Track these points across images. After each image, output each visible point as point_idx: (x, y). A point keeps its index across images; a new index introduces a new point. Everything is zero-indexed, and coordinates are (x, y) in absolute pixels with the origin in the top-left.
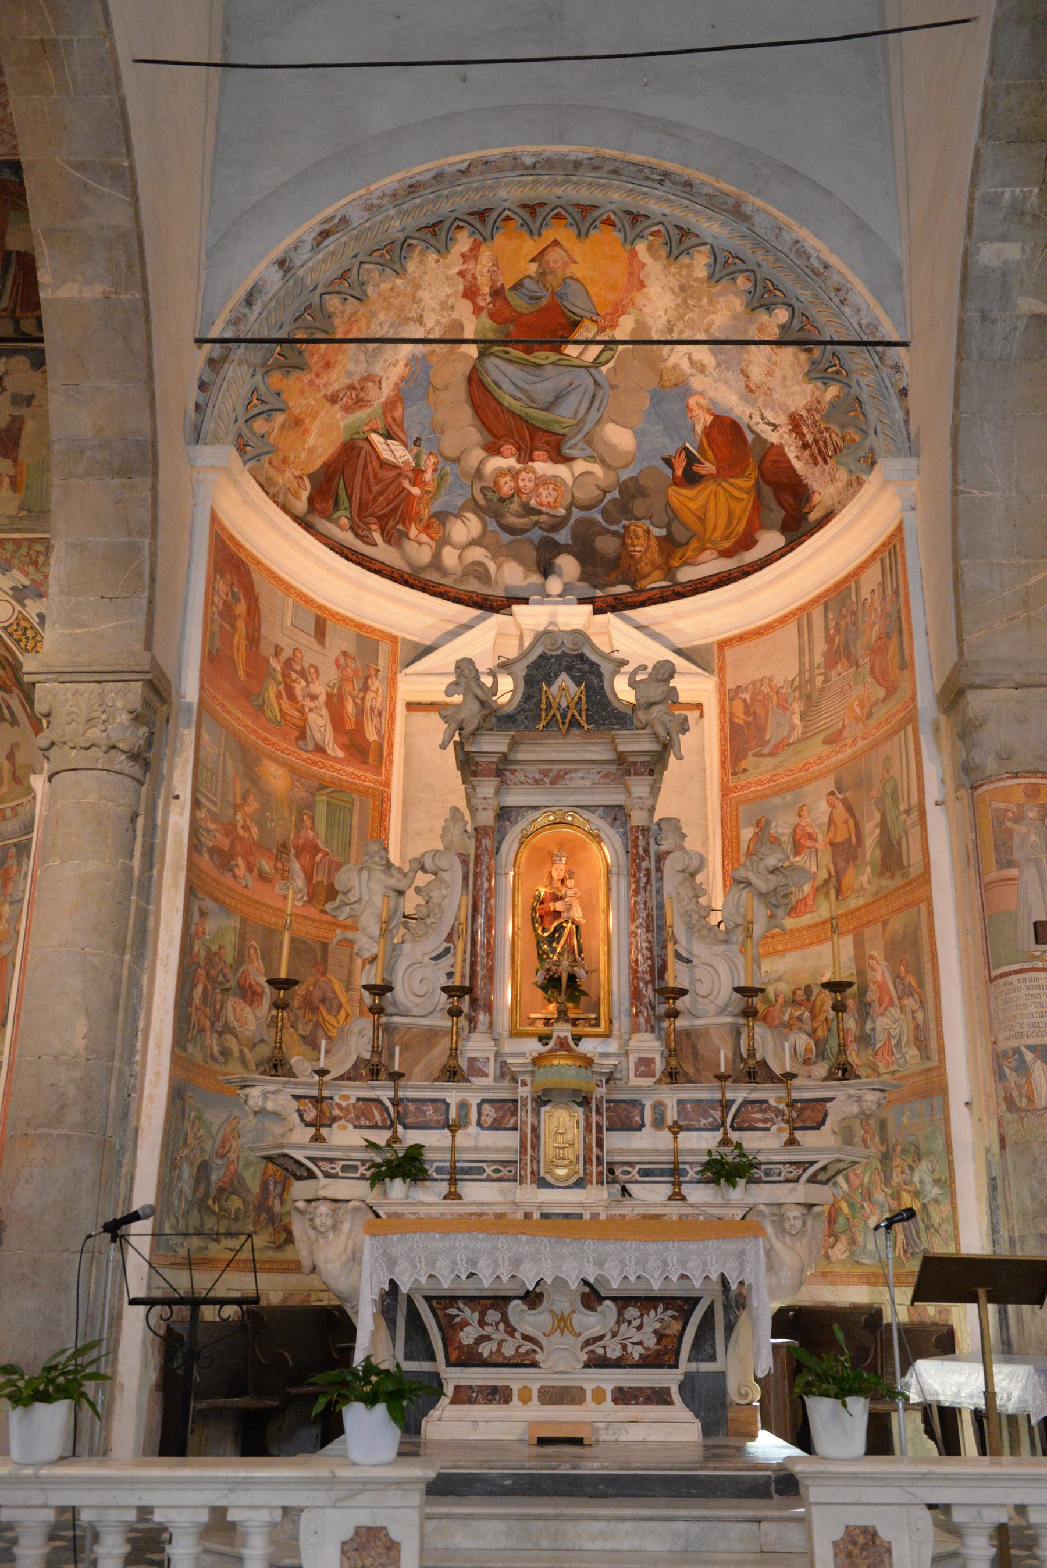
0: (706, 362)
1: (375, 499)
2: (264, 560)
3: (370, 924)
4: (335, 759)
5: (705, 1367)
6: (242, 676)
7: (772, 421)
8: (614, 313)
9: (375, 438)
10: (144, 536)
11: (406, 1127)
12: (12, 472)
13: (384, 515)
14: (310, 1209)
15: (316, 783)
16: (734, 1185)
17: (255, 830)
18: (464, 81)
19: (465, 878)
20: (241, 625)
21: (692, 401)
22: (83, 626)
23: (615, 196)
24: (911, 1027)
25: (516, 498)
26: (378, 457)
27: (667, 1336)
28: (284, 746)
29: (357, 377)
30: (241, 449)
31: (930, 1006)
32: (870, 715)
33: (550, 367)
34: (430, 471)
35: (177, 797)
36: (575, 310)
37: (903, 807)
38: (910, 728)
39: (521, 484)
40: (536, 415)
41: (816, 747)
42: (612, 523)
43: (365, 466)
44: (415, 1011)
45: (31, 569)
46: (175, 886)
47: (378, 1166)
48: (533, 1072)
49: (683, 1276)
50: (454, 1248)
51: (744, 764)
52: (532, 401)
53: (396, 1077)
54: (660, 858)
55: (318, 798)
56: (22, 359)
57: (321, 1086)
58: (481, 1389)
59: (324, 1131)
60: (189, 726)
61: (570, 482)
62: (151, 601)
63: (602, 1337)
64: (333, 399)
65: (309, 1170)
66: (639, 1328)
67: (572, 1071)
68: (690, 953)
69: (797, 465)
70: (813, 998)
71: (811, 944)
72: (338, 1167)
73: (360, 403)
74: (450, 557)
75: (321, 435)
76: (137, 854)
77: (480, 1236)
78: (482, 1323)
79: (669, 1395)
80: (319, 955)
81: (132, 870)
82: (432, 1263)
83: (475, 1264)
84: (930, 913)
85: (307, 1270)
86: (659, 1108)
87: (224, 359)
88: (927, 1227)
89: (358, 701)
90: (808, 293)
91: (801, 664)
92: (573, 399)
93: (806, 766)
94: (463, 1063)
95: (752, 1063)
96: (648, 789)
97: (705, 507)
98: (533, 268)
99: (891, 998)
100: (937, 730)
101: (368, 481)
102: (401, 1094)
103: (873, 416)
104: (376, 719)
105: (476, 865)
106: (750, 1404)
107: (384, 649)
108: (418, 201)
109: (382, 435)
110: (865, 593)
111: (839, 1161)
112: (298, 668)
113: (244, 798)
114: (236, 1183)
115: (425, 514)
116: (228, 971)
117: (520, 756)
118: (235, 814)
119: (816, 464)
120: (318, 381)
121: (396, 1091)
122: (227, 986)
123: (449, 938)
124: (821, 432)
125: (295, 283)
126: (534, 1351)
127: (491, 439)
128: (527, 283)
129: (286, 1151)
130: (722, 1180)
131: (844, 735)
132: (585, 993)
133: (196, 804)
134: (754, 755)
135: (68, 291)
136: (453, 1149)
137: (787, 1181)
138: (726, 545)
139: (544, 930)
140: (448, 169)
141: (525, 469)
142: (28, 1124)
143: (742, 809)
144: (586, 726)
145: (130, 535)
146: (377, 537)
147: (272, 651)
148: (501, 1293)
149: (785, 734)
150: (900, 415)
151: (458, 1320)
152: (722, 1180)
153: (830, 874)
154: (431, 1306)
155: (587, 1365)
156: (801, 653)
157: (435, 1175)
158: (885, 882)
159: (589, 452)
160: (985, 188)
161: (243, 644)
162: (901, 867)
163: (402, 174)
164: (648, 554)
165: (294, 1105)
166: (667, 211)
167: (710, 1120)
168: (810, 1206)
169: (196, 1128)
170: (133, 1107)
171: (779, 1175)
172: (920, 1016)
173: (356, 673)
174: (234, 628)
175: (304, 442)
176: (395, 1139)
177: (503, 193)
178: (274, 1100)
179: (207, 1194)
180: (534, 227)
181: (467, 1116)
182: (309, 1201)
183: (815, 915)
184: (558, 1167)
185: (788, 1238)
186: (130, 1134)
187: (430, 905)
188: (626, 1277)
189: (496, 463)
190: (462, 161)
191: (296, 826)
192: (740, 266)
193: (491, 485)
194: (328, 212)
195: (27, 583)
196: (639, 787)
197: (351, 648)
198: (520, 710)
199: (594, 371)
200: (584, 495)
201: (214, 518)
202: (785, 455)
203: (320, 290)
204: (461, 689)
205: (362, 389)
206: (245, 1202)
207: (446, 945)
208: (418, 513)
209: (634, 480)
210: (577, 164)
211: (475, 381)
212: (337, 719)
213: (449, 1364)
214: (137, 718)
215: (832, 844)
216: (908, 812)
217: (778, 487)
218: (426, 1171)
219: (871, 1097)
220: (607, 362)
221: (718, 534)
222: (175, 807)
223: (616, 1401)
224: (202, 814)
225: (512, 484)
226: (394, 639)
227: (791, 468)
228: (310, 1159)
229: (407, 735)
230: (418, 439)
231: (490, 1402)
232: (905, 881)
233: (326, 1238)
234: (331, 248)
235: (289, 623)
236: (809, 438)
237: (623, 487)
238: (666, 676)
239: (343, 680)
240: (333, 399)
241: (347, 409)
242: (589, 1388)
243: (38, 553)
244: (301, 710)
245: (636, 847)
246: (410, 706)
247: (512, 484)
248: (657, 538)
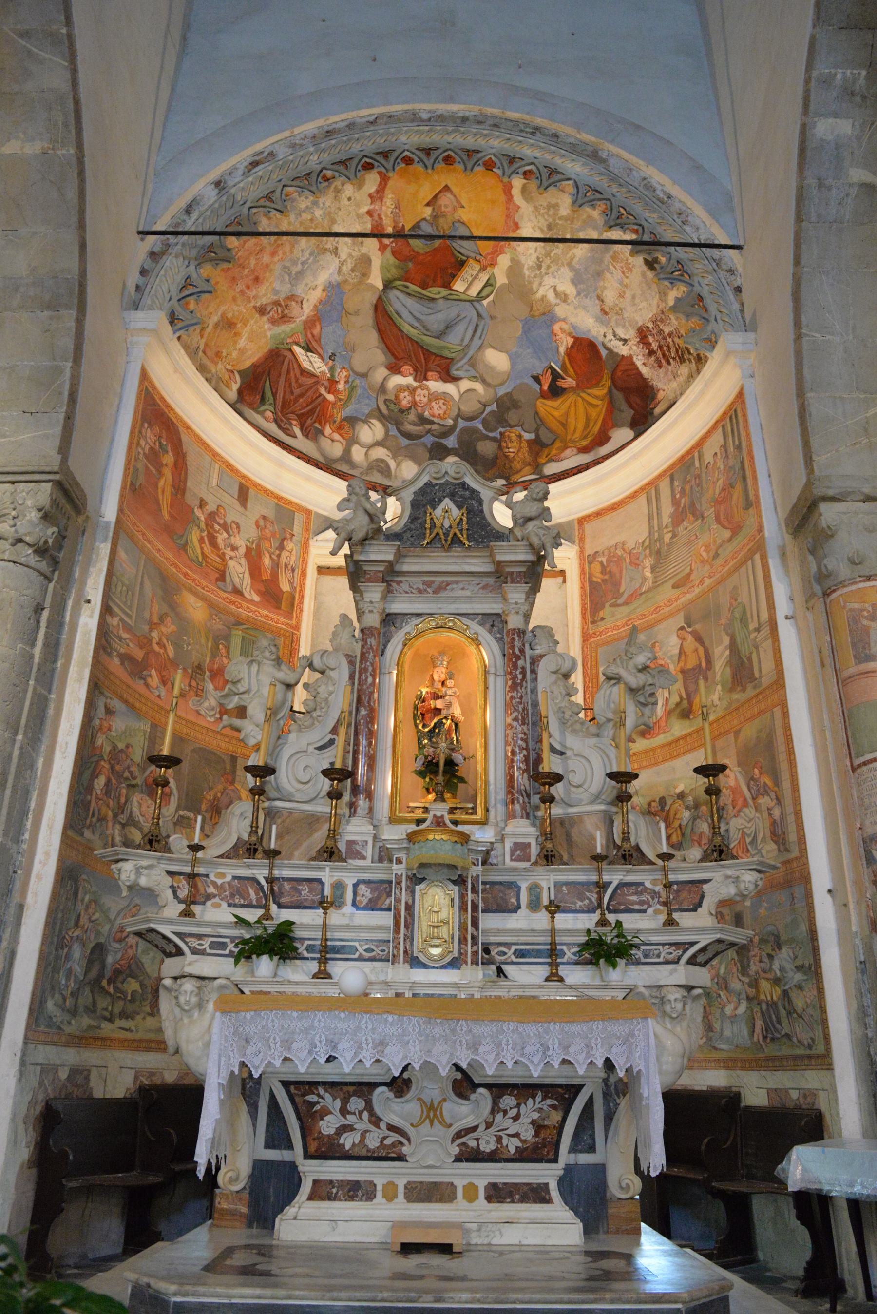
0: (568, 292)
1: (296, 400)
2: (194, 427)
3: (257, 712)
4: (251, 601)
5: (584, 1159)
6: (166, 516)
7: (623, 336)
8: (493, 253)
9: (297, 350)
11: (280, 906)
13: (303, 414)
14: (175, 987)
15: (232, 619)
16: (614, 966)
17: (171, 650)
18: (374, 60)
19: (352, 677)
20: (168, 473)
21: (556, 327)
23: (495, 143)
24: (767, 824)
25: (413, 410)
26: (299, 366)
27: (545, 1127)
28: (205, 583)
29: (282, 296)
30: (173, 319)
31: (788, 802)
32: (716, 556)
33: (441, 301)
34: (342, 382)
35: (89, 601)
36: (462, 251)
37: (752, 627)
38: (757, 557)
39: (417, 398)
40: (429, 341)
41: (667, 592)
42: (491, 431)
43: (288, 372)
44: (298, 796)
46: (79, 680)
47: (245, 942)
48: (407, 849)
49: (565, 1062)
50: (313, 1028)
51: (601, 614)
52: (427, 330)
53: (272, 854)
54: (535, 661)
55: (234, 632)
57: (195, 862)
58: (342, 1184)
59: (196, 909)
60: (105, 541)
61: (457, 398)
62: (69, 418)
63: (474, 1129)
64: (262, 311)
65: (176, 946)
66: (516, 1118)
67: (448, 846)
68: (564, 746)
69: (645, 371)
70: (667, 808)
71: (665, 760)
72: (206, 943)
73: (284, 318)
74: (358, 454)
75: (250, 339)
76: (39, 643)
77: (342, 1015)
78: (344, 1112)
79: (548, 1192)
80: (228, 767)
81: (32, 657)
82: (288, 1044)
83: (335, 1045)
84: (786, 715)
85: (171, 1050)
86: (534, 889)
87: (163, 253)
88: (789, 1014)
89: (274, 557)
90: (655, 215)
91: (651, 527)
92: (460, 329)
93: (657, 609)
94: (342, 846)
95: (626, 846)
96: (523, 596)
97: (567, 414)
98: (428, 211)
99: (745, 800)
100: (783, 555)
101: (290, 384)
102: (276, 873)
103: (713, 308)
104: (289, 574)
105: (361, 663)
106: (632, 1198)
107: (299, 518)
108: (333, 142)
109: (303, 348)
110: (708, 458)
111: (719, 941)
112: (222, 522)
113: (162, 618)
114: (133, 966)
115: (338, 418)
116: (134, 769)
117: (405, 568)
118: (151, 630)
119: (660, 366)
120: (248, 293)
121: (271, 869)
122: (134, 782)
123: (334, 731)
124: (665, 338)
125: (228, 199)
126: (401, 1143)
127: (393, 360)
128: (423, 225)
129: (152, 925)
130: (602, 961)
131: (692, 577)
132: (462, 780)
133: (106, 610)
134: (611, 606)
136: (325, 927)
137: (667, 962)
138: (584, 443)
139: (424, 726)
140: (358, 120)
141: (420, 387)
143: (600, 650)
144: (467, 543)
145: (54, 359)
146: (297, 430)
147: (198, 503)
148: (366, 1079)
149: (638, 586)
150: (736, 306)
151: (318, 1107)
152: (602, 961)
153: (681, 698)
154: (288, 1092)
155: (458, 1159)
156: (650, 518)
157: (306, 954)
158: (735, 696)
159: (473, 373)
160: (822, 69)
161: (169, 490)
162: (752, 678)
163: (320, 122)
164: (520, 454)
165: (168, 880)
166: (538, 155)
167: (586, 902)
168: (690, 988)
169: (90, 911)
170: (17, 885)
171: (658, 956)
172: (776, 813)
173: (273, 534)
174: (161, 474)
175: (236, 342)
176: (267, 916)
177: (403, 139)
178: (148, 876)
179: (101, 976)
180: (429, 163)
181: (342, 896)
182: (175, 978)
183: (668, 734)
184: (431, 946)
185: (667, 1020)
186: (12, 910)
187: (317, 699)
188: (502, 1062)
189: (397, 380)
190: (370, 115)
191: (212, 653)
192: (598, 196)
193: (393, 398)
194: (258, 147)
196: (516, 594)
197: (271, 514)
198: (407, 529)
199: (475, 304)
200: (469, 408)
201: (144, 375)
202: (634, 364)
203: (248, 205)
204: (352, 505)
205: (286, 306)
206: (142, 985)
207: (330, 736)
208: (332, 416)
209: (509, 395)
210: (464, 120)
211: (380, 309)
212: (255, 570)
213: (307, 1156)
214: (46, 517)
215: (683, 671)
216: (758, 630)
217: (626, 391)
218: (296, 949)
219: (749, 878)
220: (488, 296)
221: (577, 435)
222: (85, 610)
223: (489, 1199)
224: (114, 621)
225: (410, 398)
226: (308, 512)
227: (640, 374)
228: (178, 934)
229: (317, 596)
230: (333, 354)
231: (352, 1198)
232: (757, 691)
233: (191, 1017)
234: (260, 173)
235: (214, 484)
236: (655, 346)
237: (500, 401)
238: (541, 495)
239: (262, 538)
240: (262, 311)
241: (274, 322)
242: (460, 1184)
244: (222, 556)
245: (513, 647)
246: (322, 570)
247: (410, 398)
248: (528, 441)
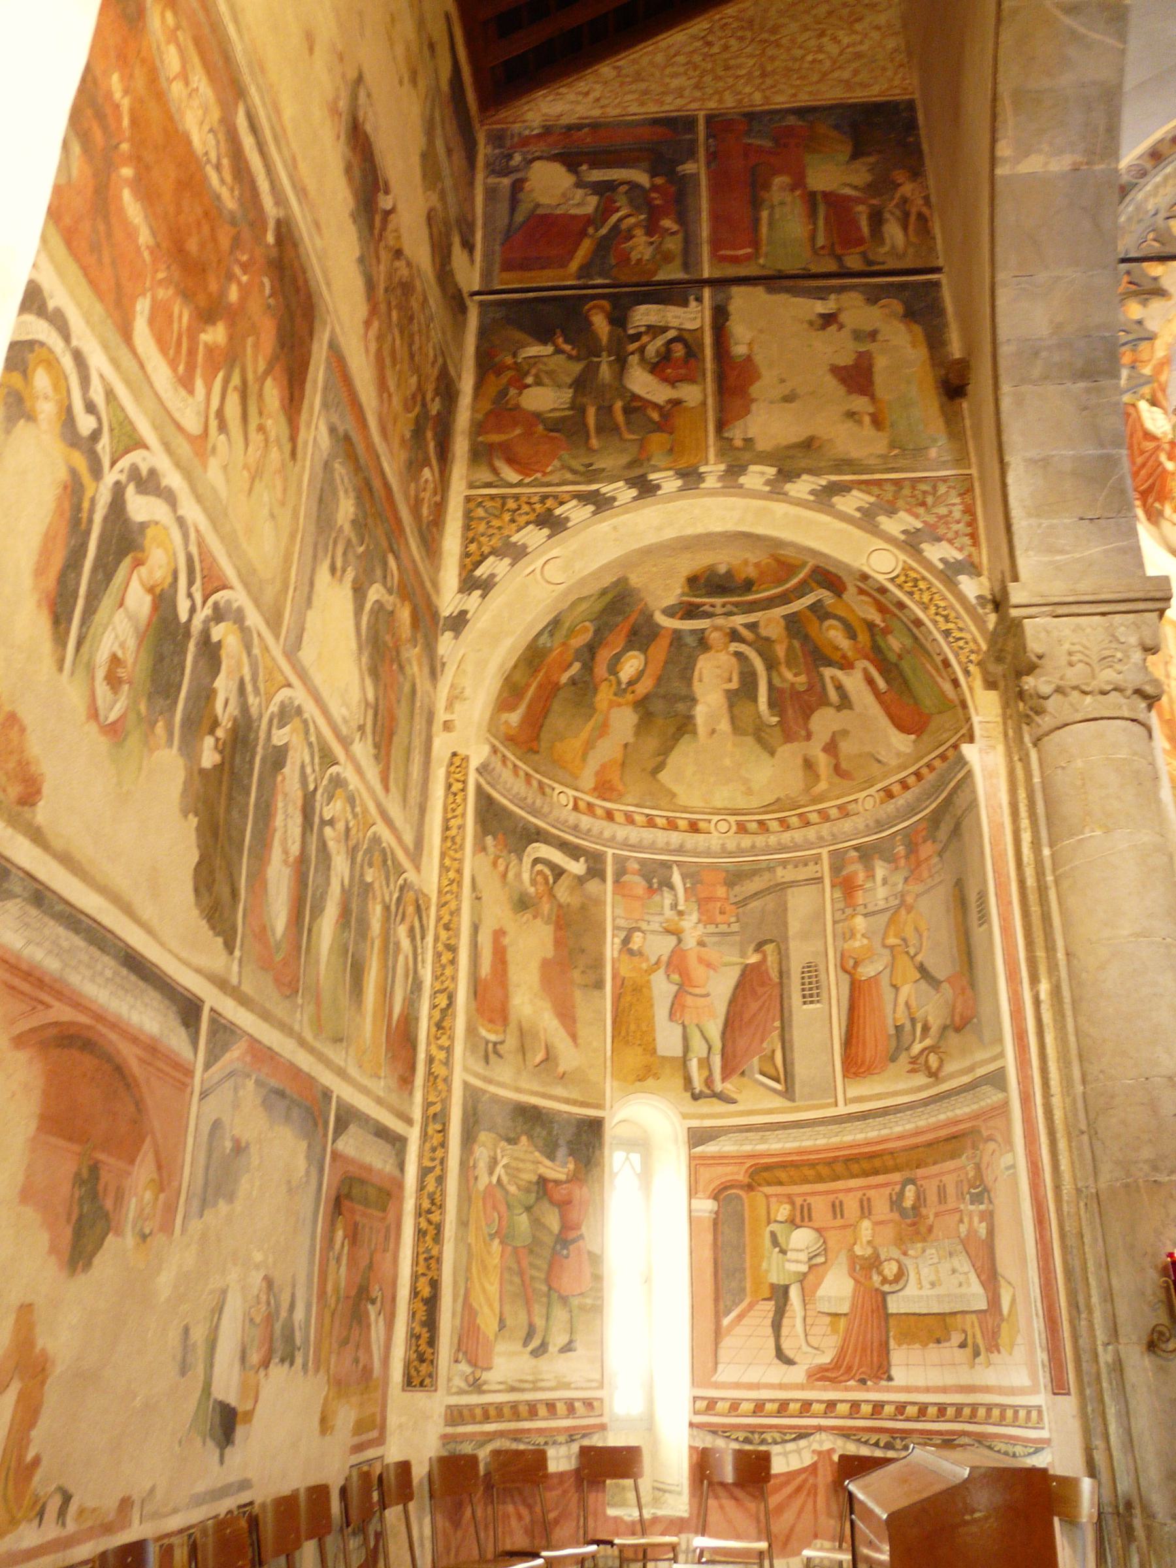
10: (1119, 446)
12: (871, 410)
22: (1062, 552)
45: (921, 510)
135: (1032, 165)
142: (1155, 1168)
145: (1102, 446)
195: (919, 525)
243: (925, 493)
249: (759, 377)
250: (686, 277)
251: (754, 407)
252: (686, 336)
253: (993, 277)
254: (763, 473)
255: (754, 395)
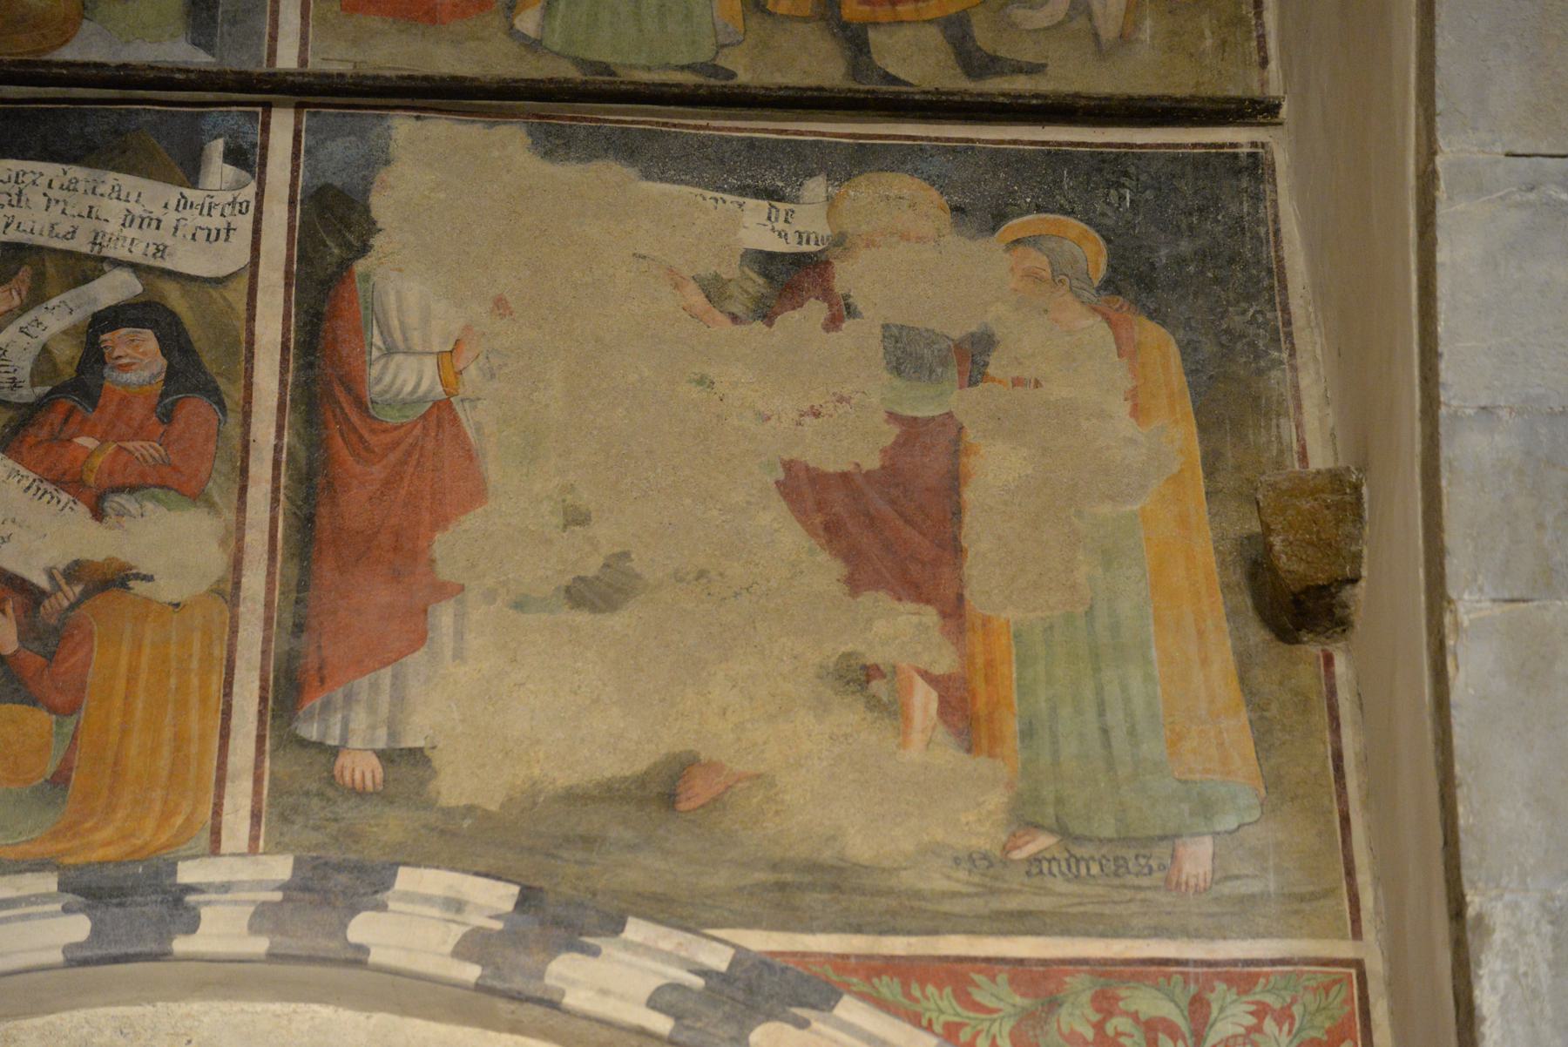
12: (945, 662)
56: (903, 185)
249: (477, 494)
250: (201, 59)
251: (444, 617)
252: (175, 298)
253: (1429, 150)
254: (456, 905)
255: (444, 572)
